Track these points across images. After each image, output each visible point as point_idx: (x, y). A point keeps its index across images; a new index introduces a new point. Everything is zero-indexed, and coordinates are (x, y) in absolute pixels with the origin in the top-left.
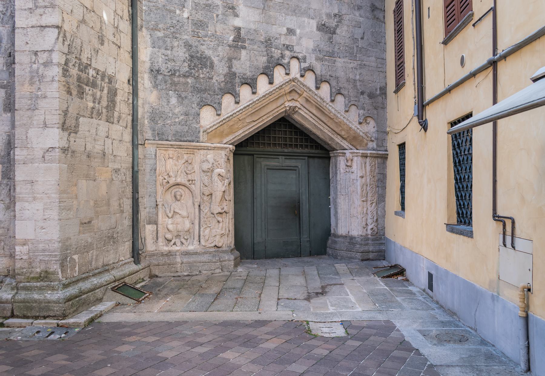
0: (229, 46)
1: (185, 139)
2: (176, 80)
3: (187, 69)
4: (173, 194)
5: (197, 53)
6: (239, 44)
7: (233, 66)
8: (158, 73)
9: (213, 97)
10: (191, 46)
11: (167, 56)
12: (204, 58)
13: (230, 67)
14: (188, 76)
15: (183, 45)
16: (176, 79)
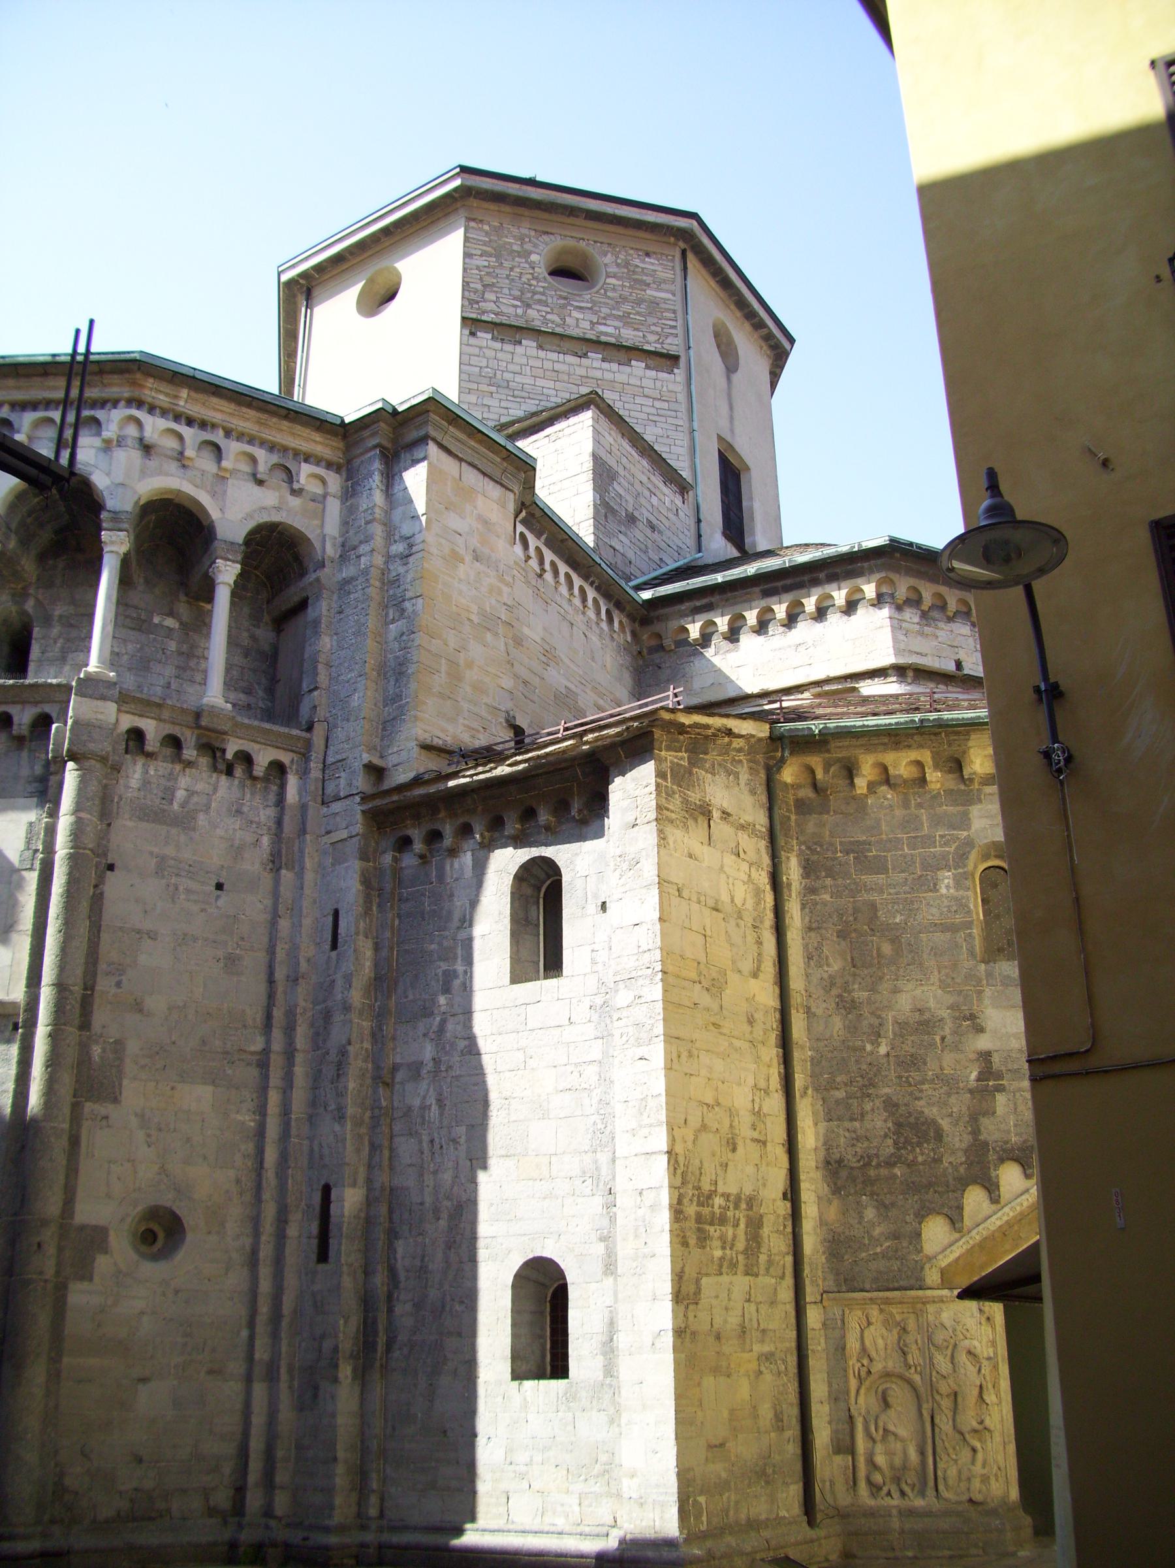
0: (971, 1091)
1: (896, 1285)
2: (872, 1175)
3: (892, 1150)
5: (908, 1117)
6: (990, 1083)
7: (982, 1129)
8: (839, 1165)
9: (945, 1196)
10: (896, 1105)
11: (854, 1132)
12: (923, 1124)
13: (976, 1132)
14: (893, 1165)
15: (881, 1106)
16: (872, 1173)
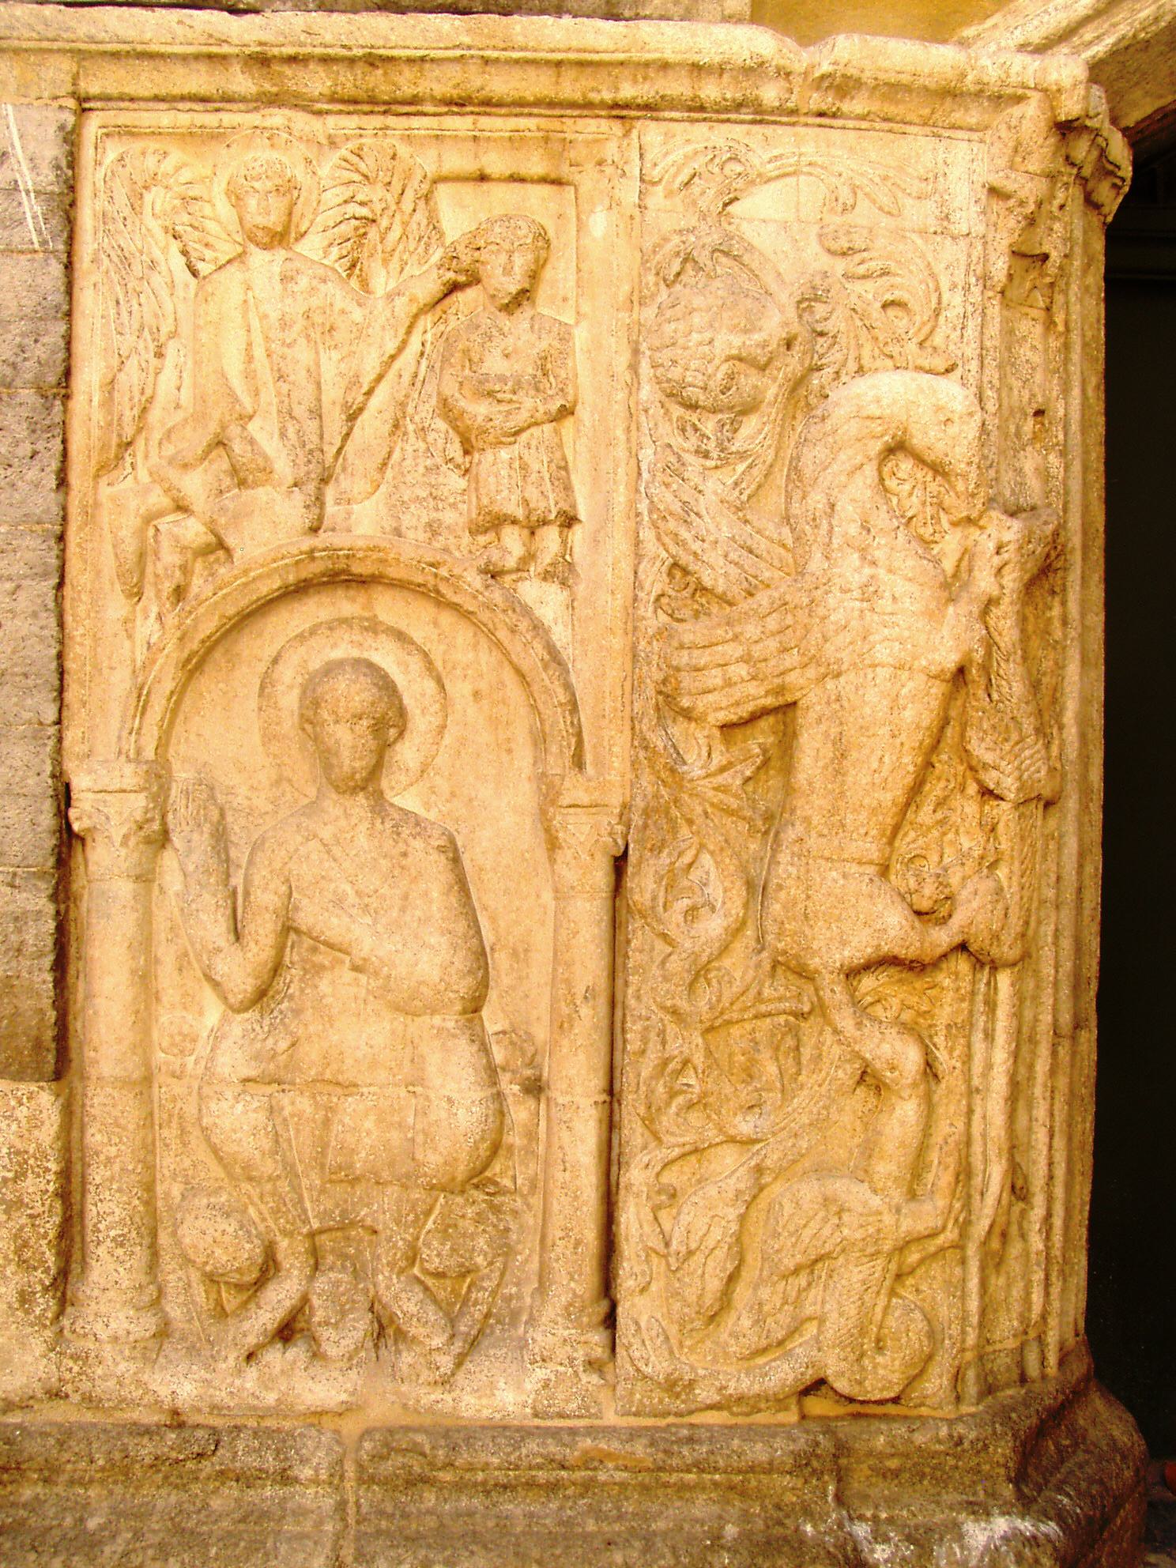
4: (289, 700)
